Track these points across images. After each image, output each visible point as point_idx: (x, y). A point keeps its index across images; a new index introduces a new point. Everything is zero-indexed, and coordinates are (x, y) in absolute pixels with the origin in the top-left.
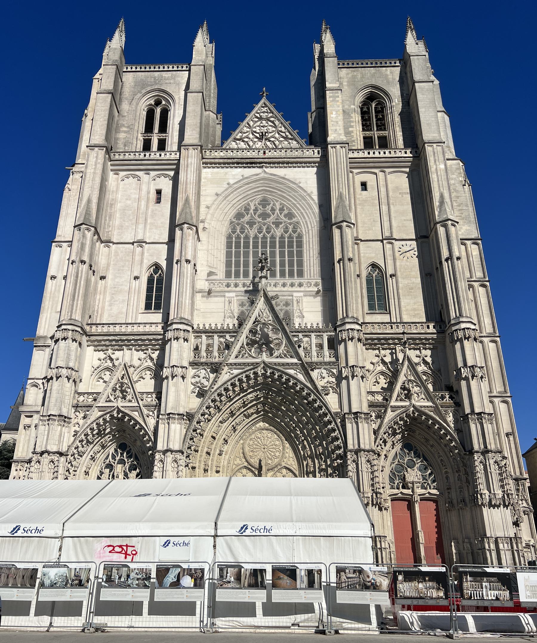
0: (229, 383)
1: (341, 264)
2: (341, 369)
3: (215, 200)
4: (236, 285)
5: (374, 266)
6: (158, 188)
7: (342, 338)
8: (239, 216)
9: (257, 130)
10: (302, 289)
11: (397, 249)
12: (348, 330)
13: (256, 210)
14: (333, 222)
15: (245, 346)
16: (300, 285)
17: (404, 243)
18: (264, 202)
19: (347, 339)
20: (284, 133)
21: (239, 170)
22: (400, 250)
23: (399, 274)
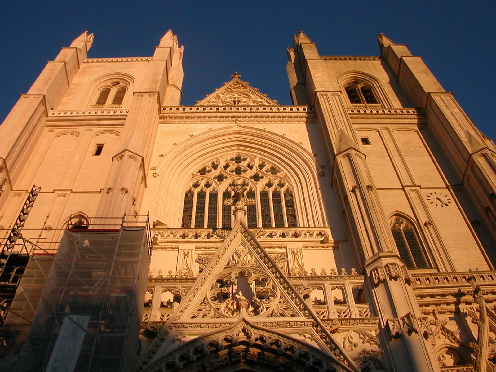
0: (177, 356)
1: (358, 193)
2: (387, 323)
3: (173, 150)
4: (196, 236)
5: (398, 215)
6: (100, 142)
7: (379, 279)
8: (203, 171)
9: (229, 100)
10: (299, 239)
11: (425, 198)
12: (387, 265)
13: (226, 167)
14: (336, 154)
15: (210, 300)
16: (296, 235)
17: (432, 191)
18: (238, 160)
19: (388, 279)
20: (261, 102)
21: (207, 125)
22: (429, 198)
23: (436, 222)
